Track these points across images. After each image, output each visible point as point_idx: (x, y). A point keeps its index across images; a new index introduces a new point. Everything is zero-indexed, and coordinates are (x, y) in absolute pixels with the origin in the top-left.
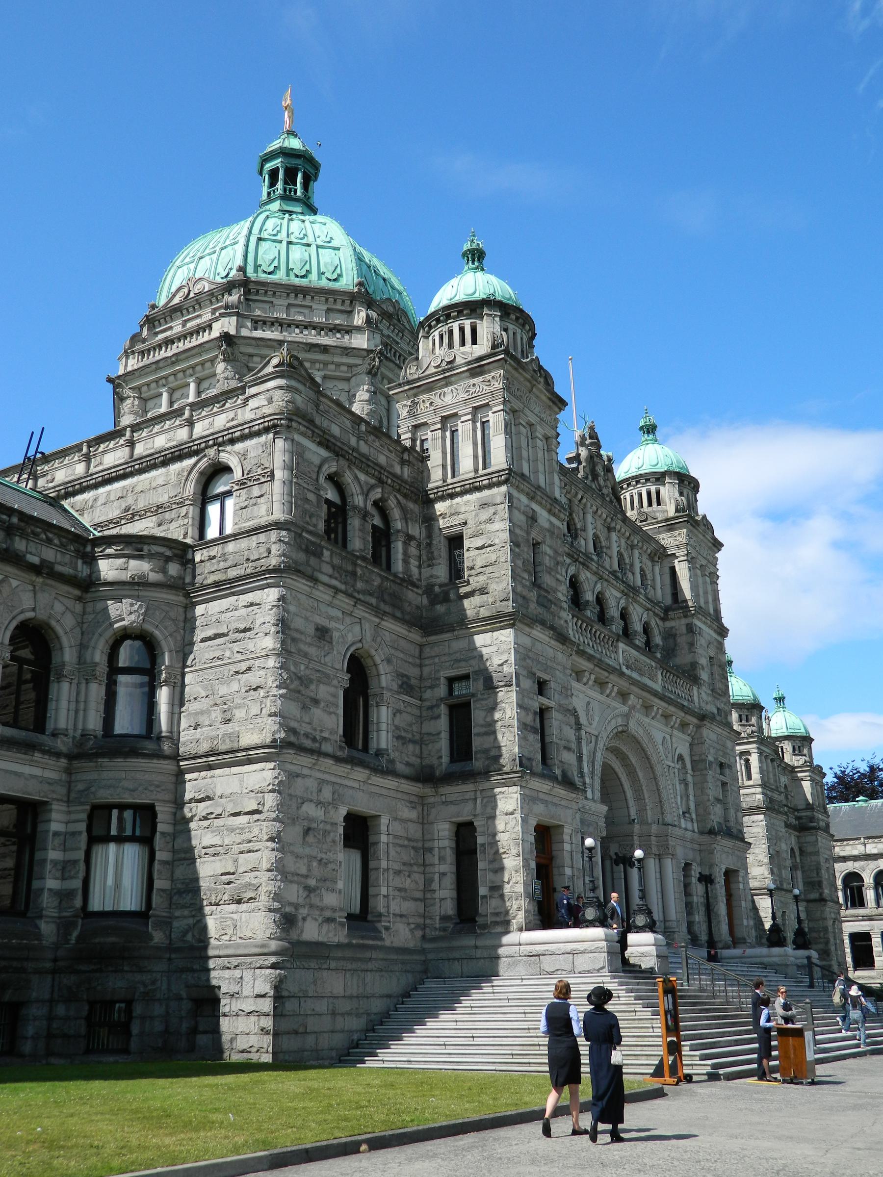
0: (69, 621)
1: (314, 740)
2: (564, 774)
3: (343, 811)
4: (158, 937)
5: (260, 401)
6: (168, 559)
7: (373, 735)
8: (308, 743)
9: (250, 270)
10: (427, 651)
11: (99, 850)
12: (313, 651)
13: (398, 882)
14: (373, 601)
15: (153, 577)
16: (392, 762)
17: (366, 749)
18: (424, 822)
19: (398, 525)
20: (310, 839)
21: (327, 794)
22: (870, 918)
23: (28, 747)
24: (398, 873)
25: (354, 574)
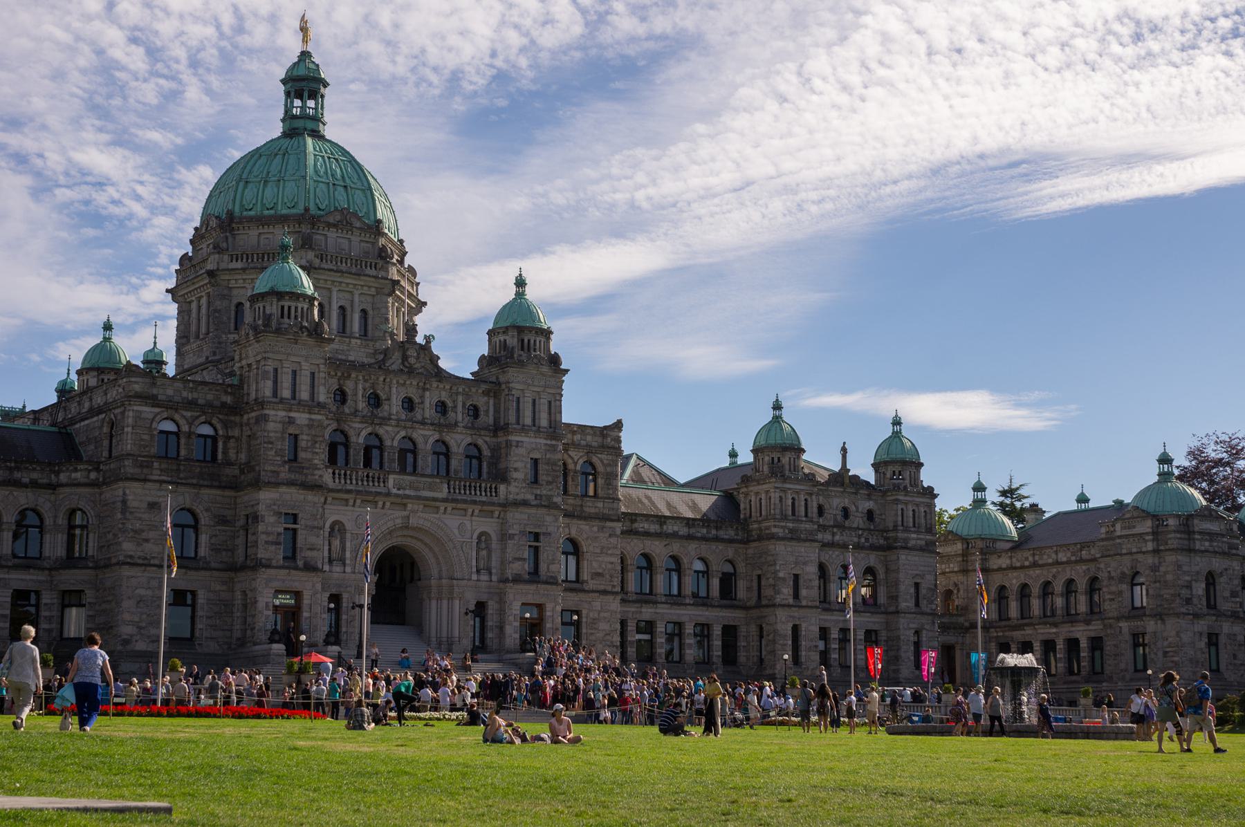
6: (90, 471)
8: (141, 562)
9: (237, 209)
11: (67, 610)
12: (145, 516)
14: (195, 481)
15: (86, 480)
19: (221, 432)
20: (141, 604)
22: (1055, 625)
24: (208, 617)
25: (178, 470)
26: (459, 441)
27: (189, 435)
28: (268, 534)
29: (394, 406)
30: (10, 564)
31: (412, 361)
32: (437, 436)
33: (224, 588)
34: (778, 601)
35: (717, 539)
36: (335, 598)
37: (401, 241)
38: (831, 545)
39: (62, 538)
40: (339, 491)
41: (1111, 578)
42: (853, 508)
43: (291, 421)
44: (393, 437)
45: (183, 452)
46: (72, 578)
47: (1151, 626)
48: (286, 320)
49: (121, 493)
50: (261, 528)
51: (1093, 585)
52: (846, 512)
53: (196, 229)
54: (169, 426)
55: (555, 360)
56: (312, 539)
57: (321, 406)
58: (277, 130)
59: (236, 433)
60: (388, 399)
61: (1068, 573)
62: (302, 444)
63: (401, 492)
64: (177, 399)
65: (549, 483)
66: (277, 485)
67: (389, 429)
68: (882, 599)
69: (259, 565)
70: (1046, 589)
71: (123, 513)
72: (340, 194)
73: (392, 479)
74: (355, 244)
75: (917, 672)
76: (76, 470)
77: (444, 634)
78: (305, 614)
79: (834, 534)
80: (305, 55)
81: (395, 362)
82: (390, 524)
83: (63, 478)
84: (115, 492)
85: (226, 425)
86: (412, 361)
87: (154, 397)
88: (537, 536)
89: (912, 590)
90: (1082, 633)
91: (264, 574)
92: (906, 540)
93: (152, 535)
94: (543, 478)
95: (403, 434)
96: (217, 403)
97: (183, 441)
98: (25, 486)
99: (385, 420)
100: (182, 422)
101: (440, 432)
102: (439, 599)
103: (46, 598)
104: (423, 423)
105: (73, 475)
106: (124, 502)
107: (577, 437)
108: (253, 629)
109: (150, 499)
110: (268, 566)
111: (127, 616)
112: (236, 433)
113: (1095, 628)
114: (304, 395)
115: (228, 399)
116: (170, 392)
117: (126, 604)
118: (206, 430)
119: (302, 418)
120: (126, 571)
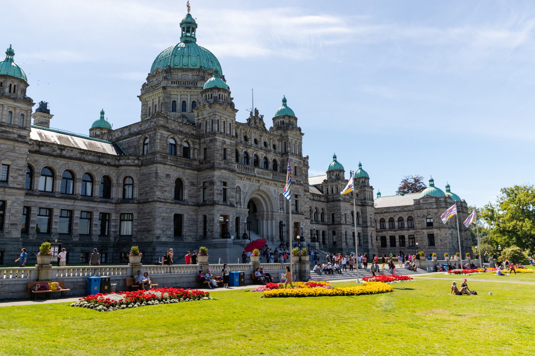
0: (114, 174)
1: (165, 199)
2: (230, 203)
3: (173, 214)
4: (134, 240)
5: (152, 124)
7: (184, 196)
8: (163, 201)
10: (199, 176)
11: (123, 223)
12: (165, 180)
13: (189, 228)
14: (183, 166)
16: (188, 202)
17: (182, 200)
18: (197, 215)
19: (192, 146)
20: (164, 220)
21: (168, 211)
22: (395, 231)
23: (106, 202)
24: (189, 226)
26: (271, 157)
28: (218, 190)
30: (99, 200)
32: (265, 155)
33: (194, 213)
34: (342, 222)
35: (320, 201)
39: (121, 189)
40: (240, 173)
41: (418, 216)
43: (224, 143)
45: (178, 153)
47: (435, 231)
48: (221, 100)
49: (155, 169)
50: (215, 187)
51: (410, 219)
53: (149, 74)
55: (300, 129)
61: (400, 215)
66: (221, 169)
67: (251, 150)
68: (361, 222)
69: (214, 204)
70: (391, 220)
71: (156, 178)
76: (129, 159)
77: (270, 234)
78: (231, 226)
80: (189, 15)
82: (254, 189)
83: (122, 162)
84: (153, 168)
85: (194, 144)
86: (258, 124)
87: (168, 128)
88: (296, 196)
90: (406, 233)
91: (217, 207)
94: (298, 174)
96: (190, 133)
97: (178, 148)
98: (106, 165)
100: (178, 140)
101: (266, 153)
102: (267, 220)
103: (113, 217)
105: (127, 161)
106: (156, 173)
108: (212, 232)
109: (167, 173)
110: (218, 204)
111: (158, 226)
113: (411, 232)
115: (194, 132)
116: (173, 127)
117: (158, 220)
119: (228, 141)
120: (158, 205)
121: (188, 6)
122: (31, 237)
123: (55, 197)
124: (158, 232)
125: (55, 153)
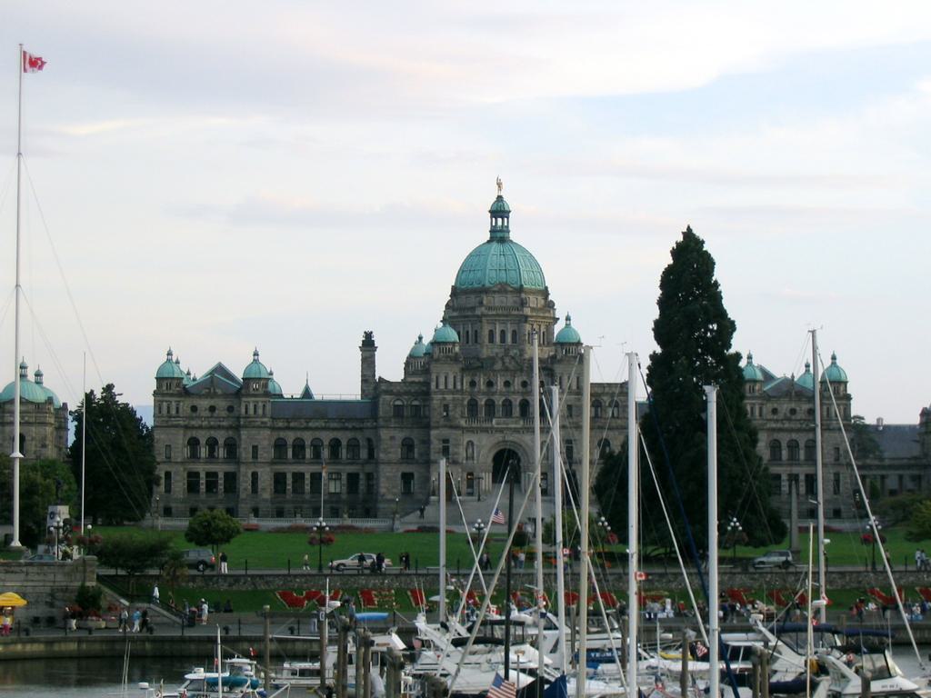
3: (400, 474)
27: (407, 407)
29: (500, 385)
31: (507, 364)
36: (471, 474)
37: (546, 288)
38: (780, 430)
42: (798, 409)
43: (444, 399)
44: (499, 400)
46: (369, 468)
52: (793, 411)
54: (398, 403)
56: (456, 450)
57: (458, 391)
58: (488, 237)
59: (427, 403)
60: (497, 383)
62: (450, 409)
63: (500, 426)
64: (402, 391)
65: (578, 416)
66: (437, 428)
72: (503, 274)
73: (494, 421)
74: (510, 300)
75: (835, 497)
79: (783, 424)
80: (500, 198)
81: (498, 366)
85: (424, 400)
86: (507, 364)
89: (832, 452)
92: (828, 425)
93: (392, 450)
94: (574, 413)
95: (504, 398)
99: (494, 394)
102: (525, 472)
104: (514, 393)
107: (607, 390)
109: (392, 435)
112: (427, 403)
114: (451, 386)
115: (424, 389)
116: (398, 388)
117: (382, 480)
118: (416, 403)
119: (449, 397)
120: (382, 467)
121: (499, 185)
122: (288, 497)
123: (304, 463)
124: (382, 490)
125: (303, 426)
